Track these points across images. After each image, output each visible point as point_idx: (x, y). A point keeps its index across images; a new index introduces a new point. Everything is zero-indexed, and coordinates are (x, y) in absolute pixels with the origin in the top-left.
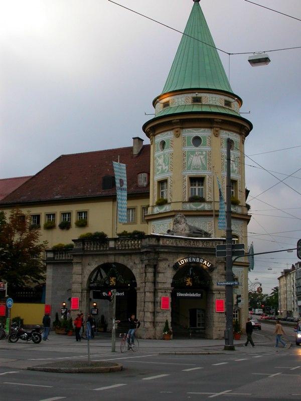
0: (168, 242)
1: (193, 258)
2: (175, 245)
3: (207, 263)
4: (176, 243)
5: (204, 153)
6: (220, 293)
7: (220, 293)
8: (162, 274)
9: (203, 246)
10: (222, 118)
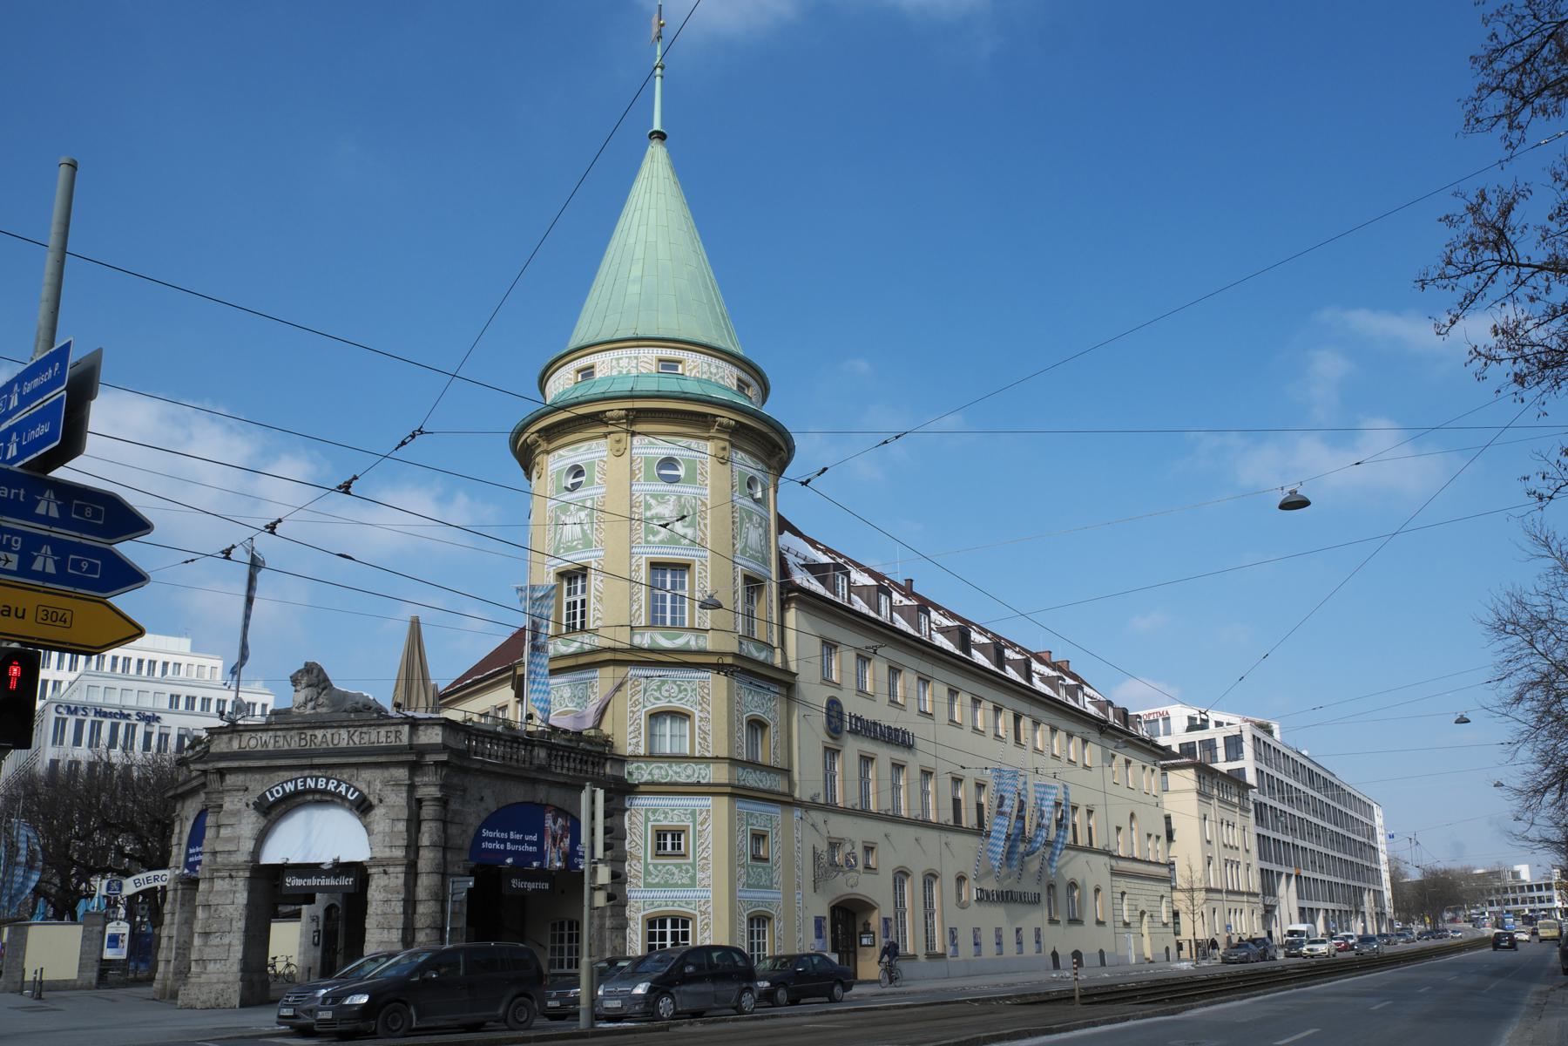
0: (253, 743)
1: (309, 780)
2: (271, 747)
3: (347, 791)
4: (276, 742)
7: (385, 872)
10: (629, 405)
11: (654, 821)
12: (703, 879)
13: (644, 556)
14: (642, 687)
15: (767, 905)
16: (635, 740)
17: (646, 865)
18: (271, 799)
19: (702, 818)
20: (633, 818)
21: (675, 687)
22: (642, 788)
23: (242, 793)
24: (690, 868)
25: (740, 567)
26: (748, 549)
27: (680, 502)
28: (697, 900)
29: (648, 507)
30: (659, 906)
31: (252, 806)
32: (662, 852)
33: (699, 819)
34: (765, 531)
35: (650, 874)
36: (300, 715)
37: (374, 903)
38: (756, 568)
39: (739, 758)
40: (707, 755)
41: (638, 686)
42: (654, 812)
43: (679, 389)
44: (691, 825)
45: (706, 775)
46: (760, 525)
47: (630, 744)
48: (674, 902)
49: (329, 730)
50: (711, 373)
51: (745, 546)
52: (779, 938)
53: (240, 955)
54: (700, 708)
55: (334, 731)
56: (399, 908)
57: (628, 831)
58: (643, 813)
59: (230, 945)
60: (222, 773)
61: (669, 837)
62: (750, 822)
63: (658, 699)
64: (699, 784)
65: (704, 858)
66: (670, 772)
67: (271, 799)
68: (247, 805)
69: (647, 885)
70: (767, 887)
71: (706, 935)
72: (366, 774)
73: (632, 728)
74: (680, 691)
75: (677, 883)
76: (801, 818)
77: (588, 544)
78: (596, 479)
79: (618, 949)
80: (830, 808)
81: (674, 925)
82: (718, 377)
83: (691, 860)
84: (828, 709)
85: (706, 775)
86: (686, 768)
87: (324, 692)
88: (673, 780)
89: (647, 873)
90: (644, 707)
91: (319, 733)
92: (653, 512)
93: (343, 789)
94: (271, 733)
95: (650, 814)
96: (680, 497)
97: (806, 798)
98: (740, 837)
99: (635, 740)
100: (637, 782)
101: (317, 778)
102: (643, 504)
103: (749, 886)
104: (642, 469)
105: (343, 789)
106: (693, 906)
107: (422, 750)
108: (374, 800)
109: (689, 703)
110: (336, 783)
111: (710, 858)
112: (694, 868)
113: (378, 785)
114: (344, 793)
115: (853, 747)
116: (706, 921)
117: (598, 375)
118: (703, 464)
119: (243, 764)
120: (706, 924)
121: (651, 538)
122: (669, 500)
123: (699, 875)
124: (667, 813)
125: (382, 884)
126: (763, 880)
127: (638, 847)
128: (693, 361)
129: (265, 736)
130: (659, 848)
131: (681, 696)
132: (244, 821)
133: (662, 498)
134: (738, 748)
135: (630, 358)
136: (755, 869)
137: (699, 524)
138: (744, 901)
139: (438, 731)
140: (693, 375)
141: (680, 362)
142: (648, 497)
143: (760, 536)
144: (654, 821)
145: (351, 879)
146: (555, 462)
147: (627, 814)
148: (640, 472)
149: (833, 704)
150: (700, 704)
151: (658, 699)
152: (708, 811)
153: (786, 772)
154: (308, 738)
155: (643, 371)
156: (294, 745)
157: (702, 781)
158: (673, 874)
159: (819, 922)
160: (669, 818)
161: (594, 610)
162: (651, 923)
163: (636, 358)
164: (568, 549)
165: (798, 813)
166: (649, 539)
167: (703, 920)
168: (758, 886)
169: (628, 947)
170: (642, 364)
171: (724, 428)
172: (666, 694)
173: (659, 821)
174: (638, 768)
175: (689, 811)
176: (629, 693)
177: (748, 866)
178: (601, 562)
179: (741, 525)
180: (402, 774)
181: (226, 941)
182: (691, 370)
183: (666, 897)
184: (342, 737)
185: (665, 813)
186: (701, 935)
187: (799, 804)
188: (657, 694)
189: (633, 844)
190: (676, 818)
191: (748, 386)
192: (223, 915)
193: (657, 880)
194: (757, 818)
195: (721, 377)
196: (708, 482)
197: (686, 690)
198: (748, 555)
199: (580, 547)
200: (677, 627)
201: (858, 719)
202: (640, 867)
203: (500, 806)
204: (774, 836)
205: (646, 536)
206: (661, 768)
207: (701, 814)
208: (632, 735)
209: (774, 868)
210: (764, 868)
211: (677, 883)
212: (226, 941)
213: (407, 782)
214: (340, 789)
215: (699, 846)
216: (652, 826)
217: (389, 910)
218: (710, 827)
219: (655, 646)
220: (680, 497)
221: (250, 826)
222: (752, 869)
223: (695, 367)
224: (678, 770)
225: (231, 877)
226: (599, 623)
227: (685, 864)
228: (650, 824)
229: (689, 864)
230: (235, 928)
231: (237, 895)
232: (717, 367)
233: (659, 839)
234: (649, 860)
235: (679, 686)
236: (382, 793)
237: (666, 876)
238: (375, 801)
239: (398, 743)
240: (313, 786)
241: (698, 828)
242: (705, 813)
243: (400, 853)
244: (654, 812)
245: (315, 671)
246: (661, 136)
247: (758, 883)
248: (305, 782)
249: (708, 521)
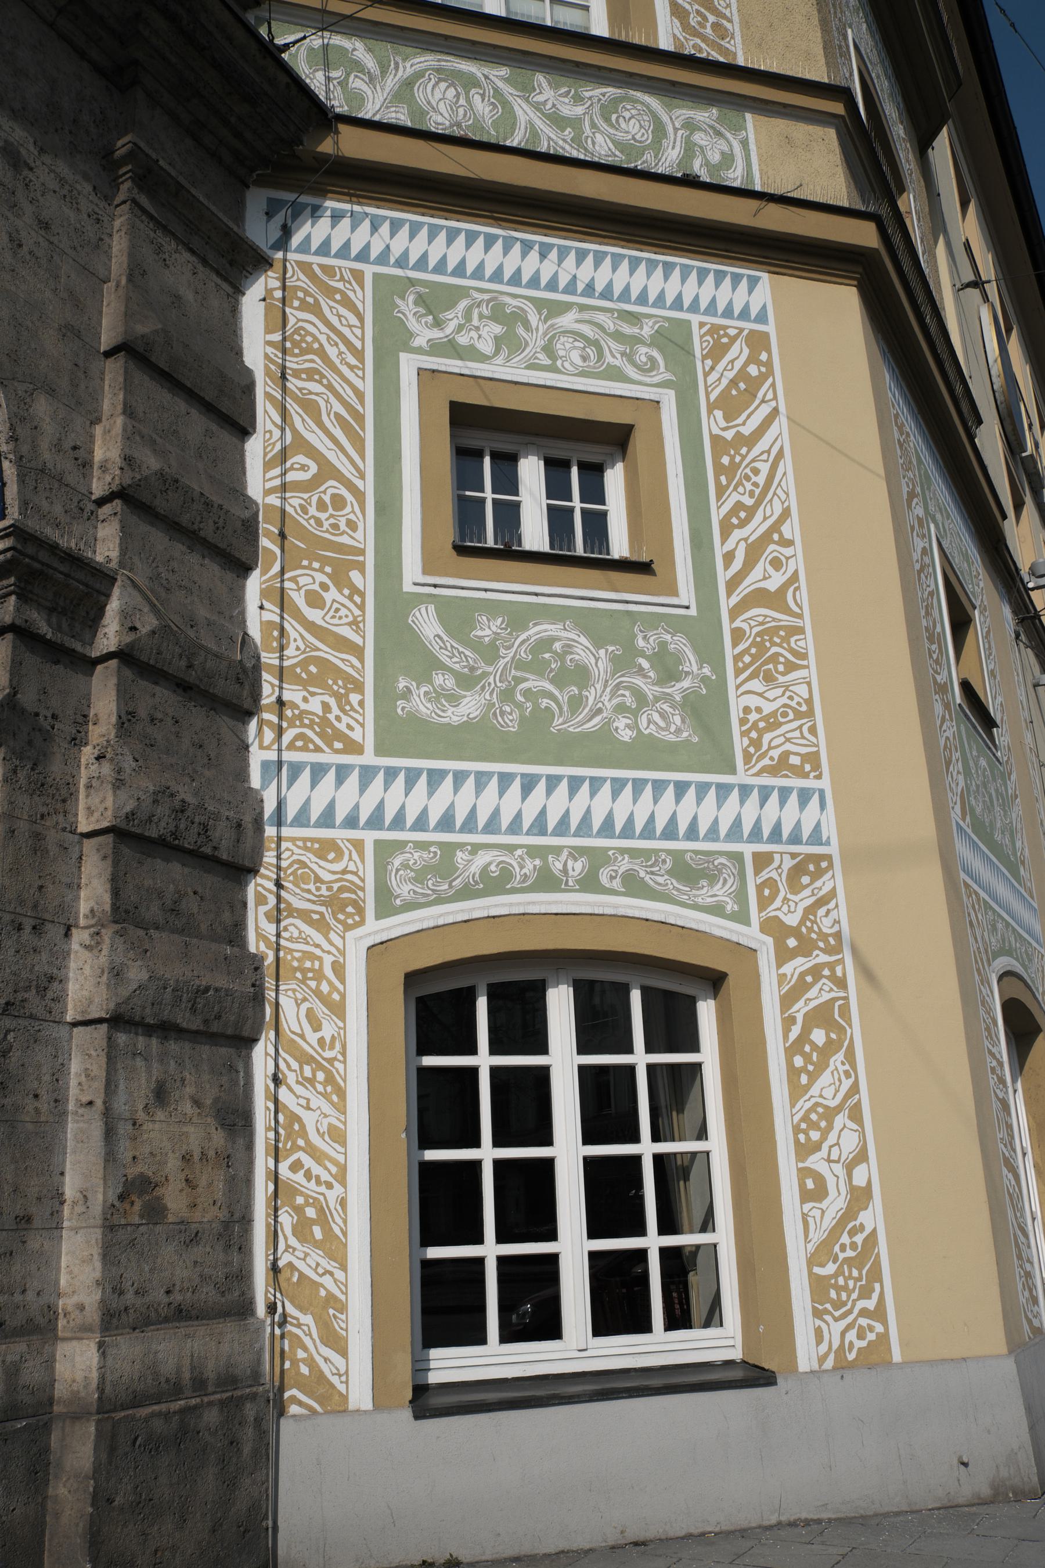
11: (435, 349)
12: (772, 722)
24: (678, 643)
28: (748, 850)
44: (669, 401)
48: (597, 858)
57: (263, 387)
58: (365, 298)
65: (760, 597)
66: (524, 113)
75: (606, 732)
83: (686, 592)
86: (608, 111)
95: (407, 307)
106: (721, 892)
112: (711, 654)
116: (820, 994)
120: (821, 1016)
124: (519, 318)
127: (332, 487)
144: (435, 349)
152: (758, 342)
158: (581, 675)
160: (535, 342)
167: (800, 988)
175: (647, 330)
183: (539, 826)
186: (796, 1092)
190: (571, 354)
206: (470, 83)
207: (717, 352)
215: (726, 530)
224: (568, 110)
227: (653, 621)
228: (408, 366)
229: (677, 625)
237: (534, 683)
241: (712, 424)
242: (739, 352)
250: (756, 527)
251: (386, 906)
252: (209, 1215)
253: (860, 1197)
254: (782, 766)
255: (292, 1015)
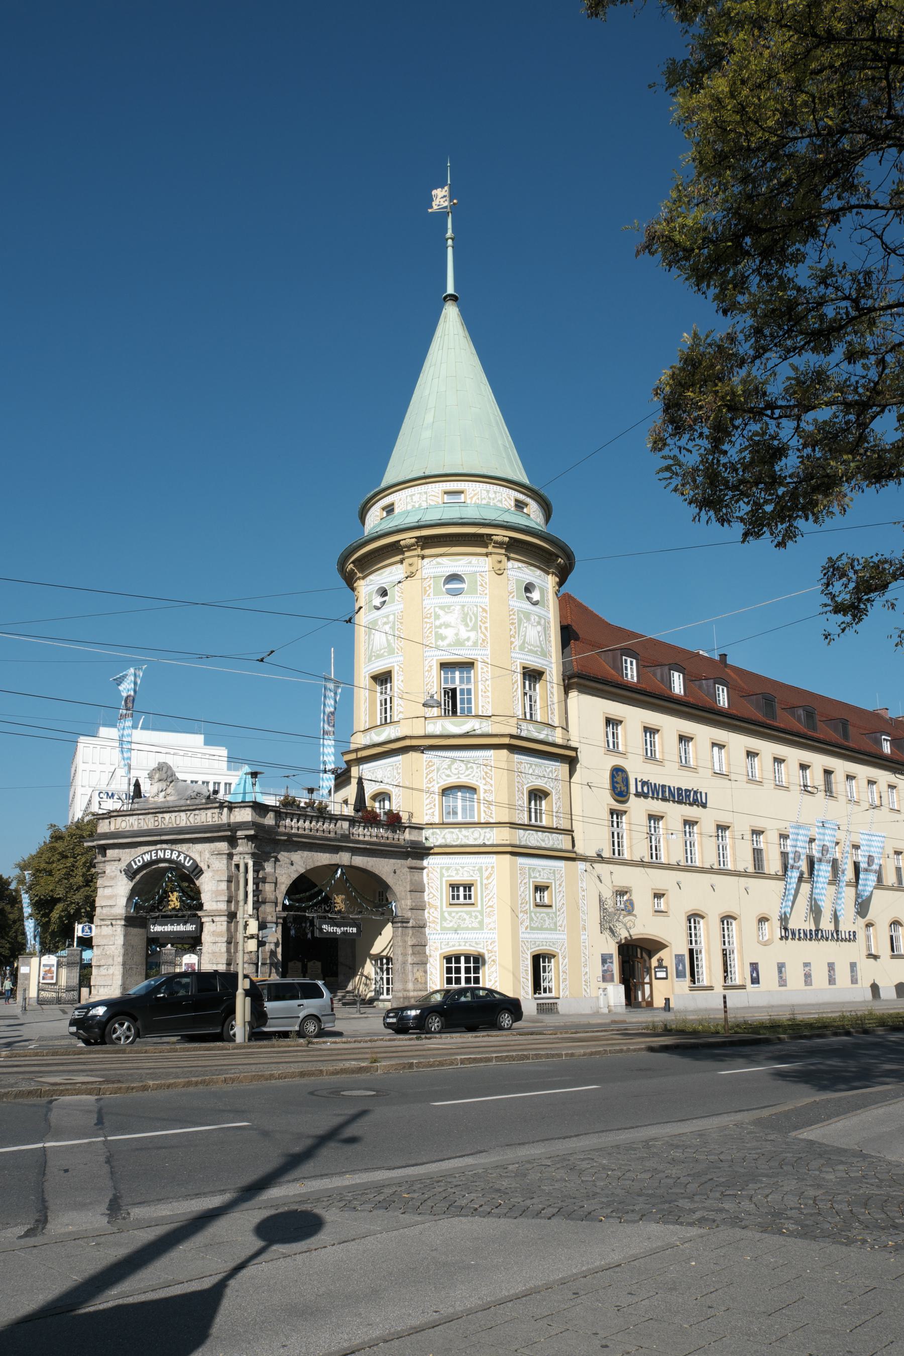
0: (124, 824)
1: (159, 851)
2: (135, 828)
5: (391, 618)
6: (213, 921)
8: (110, 889)
9: (189, 824)
11: (448, 876)
12: (490, 923)
13: (435, 658)
14: (435, 767)
15: (551, 944)
16: (432, 811)
17: (442, 912)
18: (135, 867)
19: (487, 873)
20: (430, 874)
21: (462, 765)
22: (436, 850)
23: (117, 863)
25: (519, 661)
26: (526, 645)
27: (463, 611)
29: (437, 617)
30: (454, 946)
31: (123, 873)
32: (456, 901)
33: (486, 874)
34: (545, 628)
35: (446, 920)
36: (155, 802)
37: (207, 944)
38: (535, 662)
39: (520, 822)
40: (492, 821)
41: (432, 766)
42: (448, 869)
43: (459, 516)
44: (479, 879)
45: (490, 837)
46: (539, 623)
47: (427, 814)
48: (466, 942)
49: (173, 814)
50: (490, 498)
51: (524, 642)
52: (564, 972)
53: (120, 982)
54: (484, 782)
55: (176, 814)
56: (223, 947)
57: (426, 885)
58: (439, 871)
59: (113, 974)
60: (103, 849)
61: (461, 889)
62: (533, 875)
63: (448, 776)
64: (485, 845)
65: (490, 906)
66: (460, 836)
67: (135, 867)
68: (121, 872)
69: (443, 929)
70: (551, 930)
71: (493, 969)
72: (199, 847)
73: (428, 801)
74: (467, 769)
75: (468, 927)
76: (586, 871)
77: (391, 652)
78: (397, 598)
79: (420, 980)
80: (617, 859)
81: (467, 960)
82: (496, 501)
83: (479, 908)
84: (613, 777)
85: (490, 837)
86: (473, 833)
87: (171, 785)
88: (463, 843)
89: (443, 918)
90: (438, 783)
91: (167, 816)
92: (441, 621)
93: (182, 858)
94: (135, 817)
95: (444, 871)
96: (463, 606)
97: (592, 853)
98: (522, 889)
99: (432, 811)
100: (432, 845)
101: (165, 850)
102: (433, 614)
103: (532, 929)
104: (432, 586)
105: (182, 858)
106: (481, 946)
107: (233, 828)
108: (203, 866)
109: (475, 778)
110: (177, 853)
111: (495, 906)
112: (482, 915)
113: (207, 855)
114: (182, 862)
115: (638, 808)
117: (397, 510)
118: (482, 577)
119: (116, 841)
121: (440, 643)
122: (454, 610)
123: (486, 920)
125: (212, 930)
126: (547, 924)
128: (473, 490)
129: (132, 819)
130: (453, 899)
131: (468, 772)
132: (119, 884)
133: (449, 609)
134: (519, 814)
135: (420, 493)
136: (538, 915)
137: (480, 628)
138: (527, 941)
139: (248, 811)
140: (473, 502)
141: (462, 492)
142: (437, 609)
143: (539, 632)
144: (448, 876)
145: (194, 926)
146: (366, 587)
147: (425, 871)
148: (430, 588)
149: (618, 773)
150: (484, 779)
151: (448, 776)
152: (493, 867)
153: (570, 832)
154: (160, 820)
155: (432, 503)
156: (151, 826)
157: (487, 843)
158: (465, 919)
159: (605, 959)
160: (460, 873)
161: (398, 705)
162: (448, 959)
163: (426, 493)
164: (379, 656)
165: (581, 866)
166: (438, 643)
168: (541, 929)
169: (428, 979)
170: (431, 497)
171: (500, 545)
172: (456, 772)
173: (452, 876)
174: (433, 834)
175: (477, 868)
176: (425, 772)
177: (531, 912)
178: (402, 666)
179: (519, 625)
180: (223, 846)
181: (111, 971)
182: (472, 498)
184: (182, 818)
185: (456, 870)
187: (584, 859)
188: (448, 772)
189: (431, 896)
190: (465, 873)
191: (526, 505)
192: (108, 953)
193: (451, 925)
194: (539, 872)
195: (499, 501)
196: (487, 591)
197: (472, 767)
198: (526, 650)
199: (386, 654)
200: (468, 714)
201: (644, 783)
202: (437, 914)
203: (309, 868)
204: (557, 887)
205: (436, 641)
207: (486, 870)
208: (428, 807)
209: (558, 913)
210: (548, 914)
211: (468, 927)
212: (111, 971)
213: (227, 852)
214: (180, 858)
216: (447, 881)
217: (217, 950)
218: (495, 882)
219: (445, 733)
220: (463, 606)
221: (124, 887)
222: (535, 915)
223: (475, 494)
224: (467, 834)
225: (112, 924)
226: (401, 716)
227: (474, 911)
228: (444, 879)
229: (478, 911)
230: (116, 963)
231: (117, 938)
232: (495, 493)
233: (453, 891)
234: (444, 909)
235: (466, 765)
236: (210, 861)
238: (204, 867)
239: (220, 822)
240: (162, 857)
241: (485, 882)
243: (223, 906)
244: (448, 869)
245: (165, 769)
246: (454, 298)
247: (542, 926)
248: (157, 853)
249: (488, 625)
250: (489, 897)
251: (441, 949)
252: (423, 982)
253: (496, 982)
254: (491, 929)
255: (431, 961)
